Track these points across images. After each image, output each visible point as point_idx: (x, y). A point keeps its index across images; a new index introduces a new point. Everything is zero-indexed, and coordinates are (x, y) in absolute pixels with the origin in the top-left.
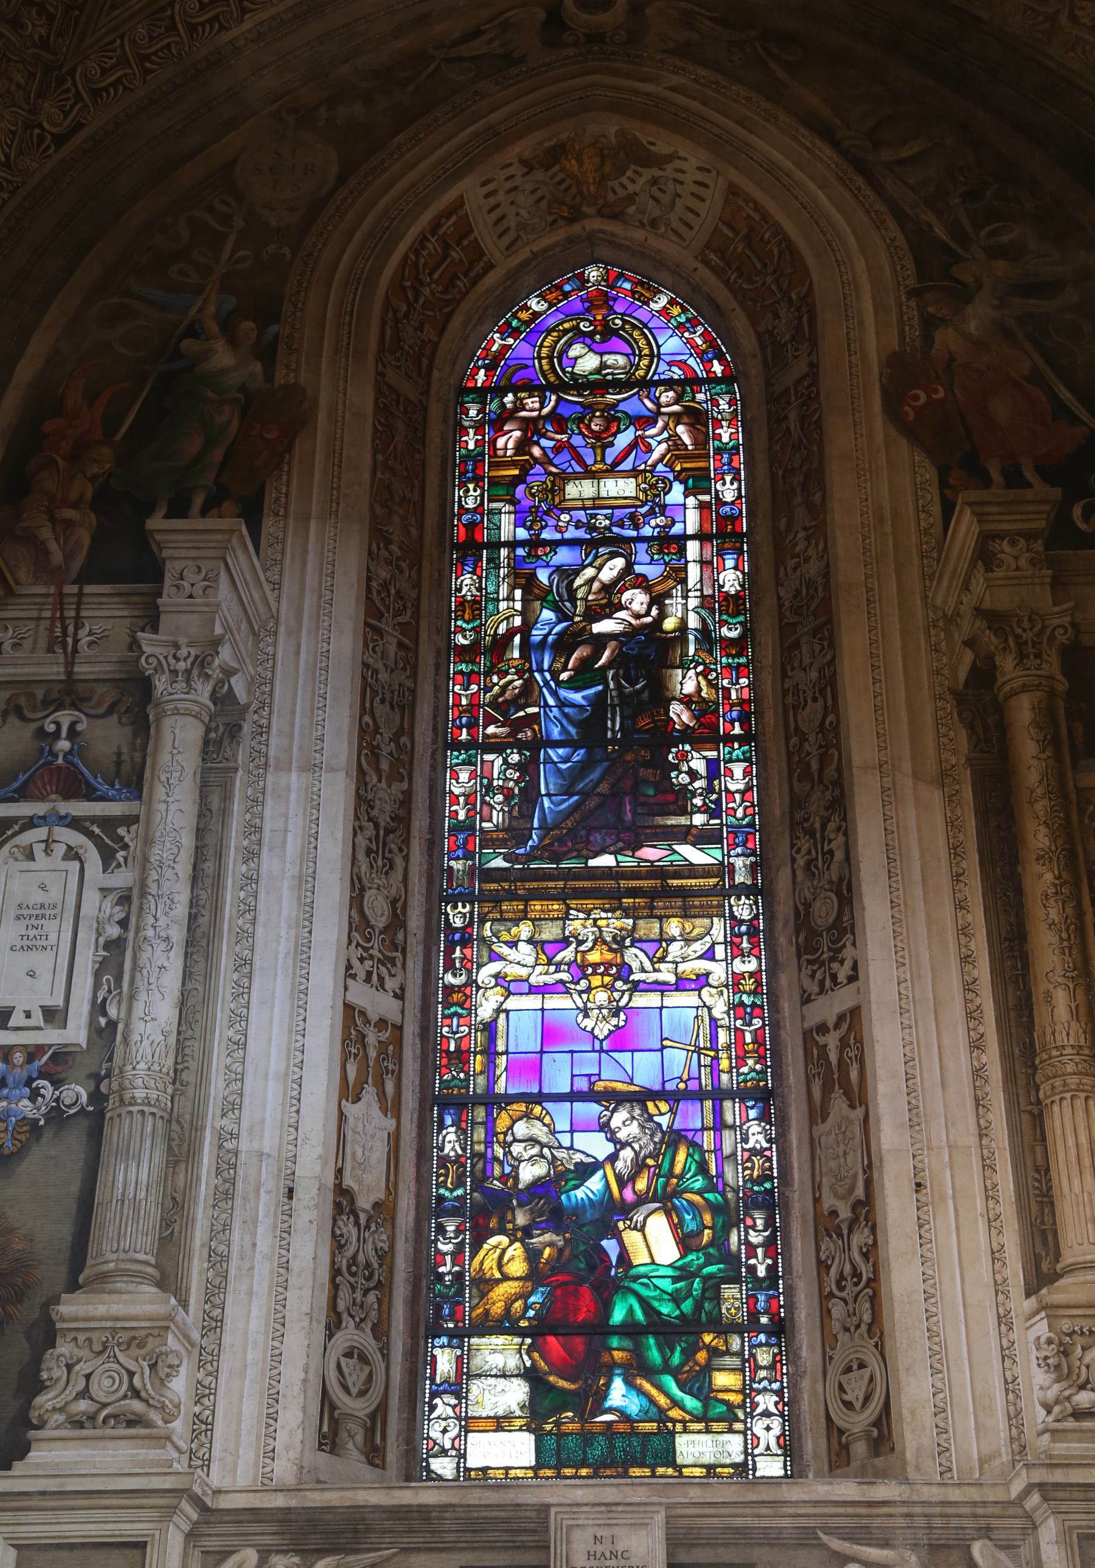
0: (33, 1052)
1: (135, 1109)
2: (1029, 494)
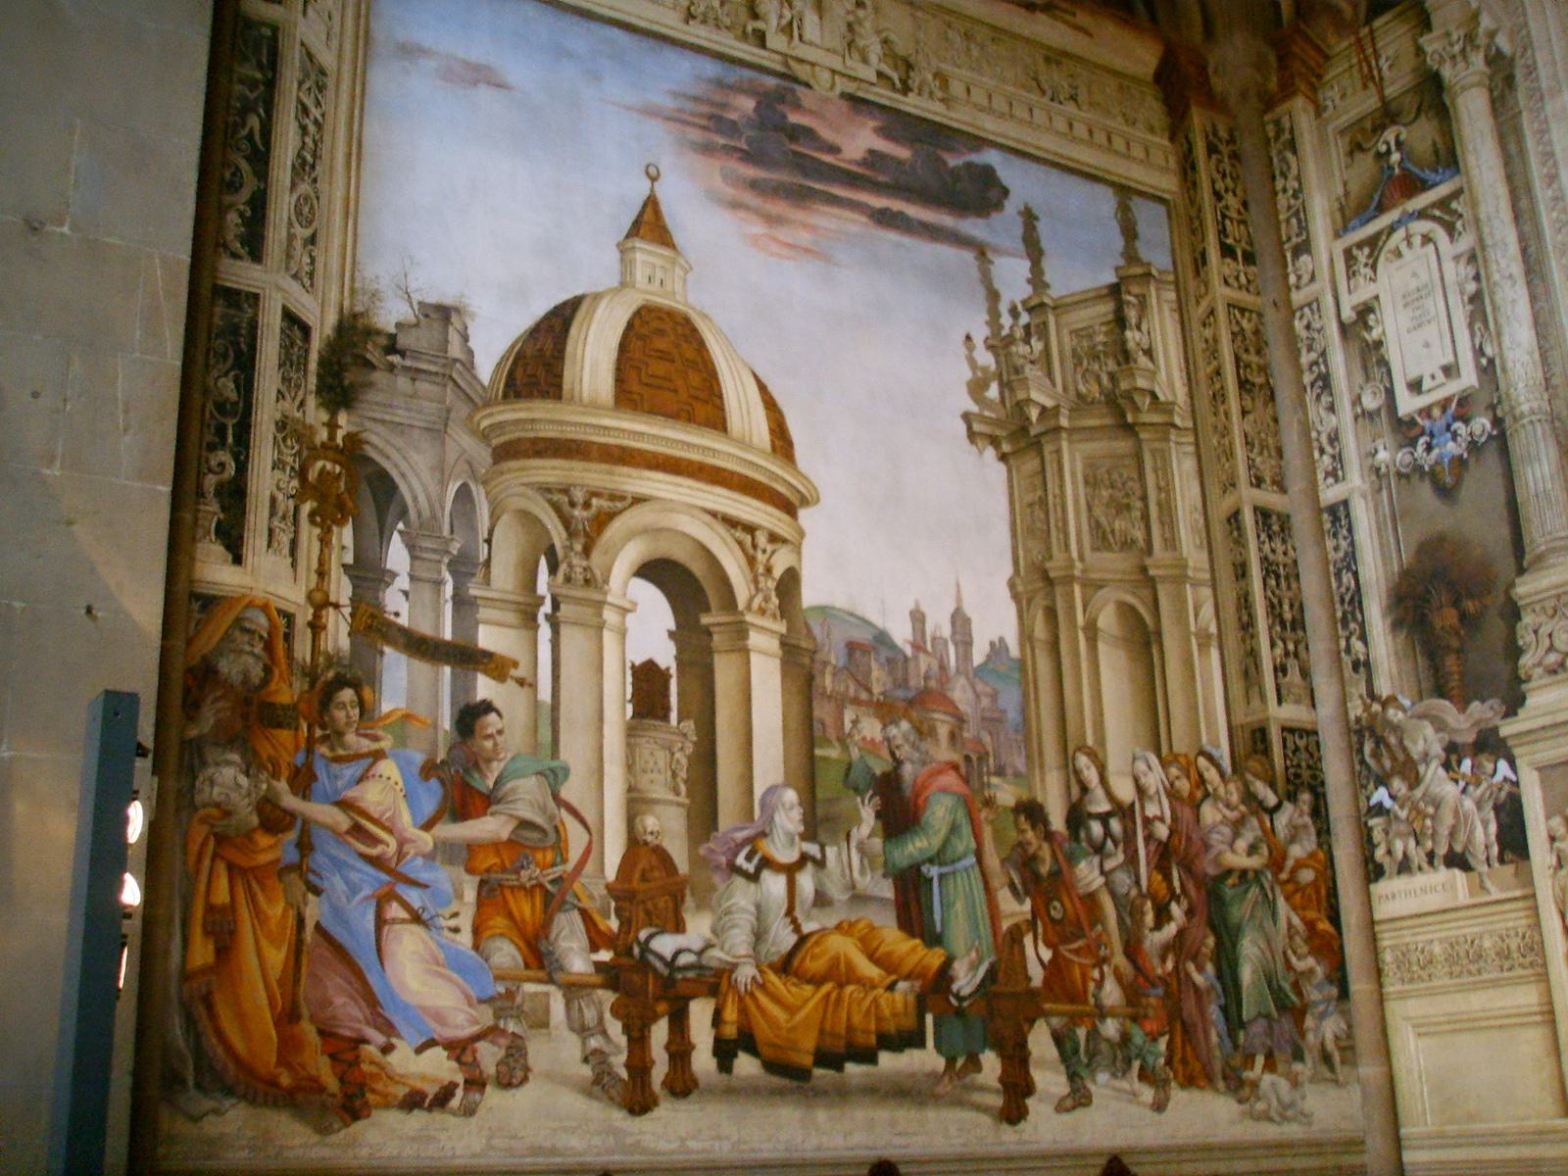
0: (1444, 405)
1: (1525, 421)
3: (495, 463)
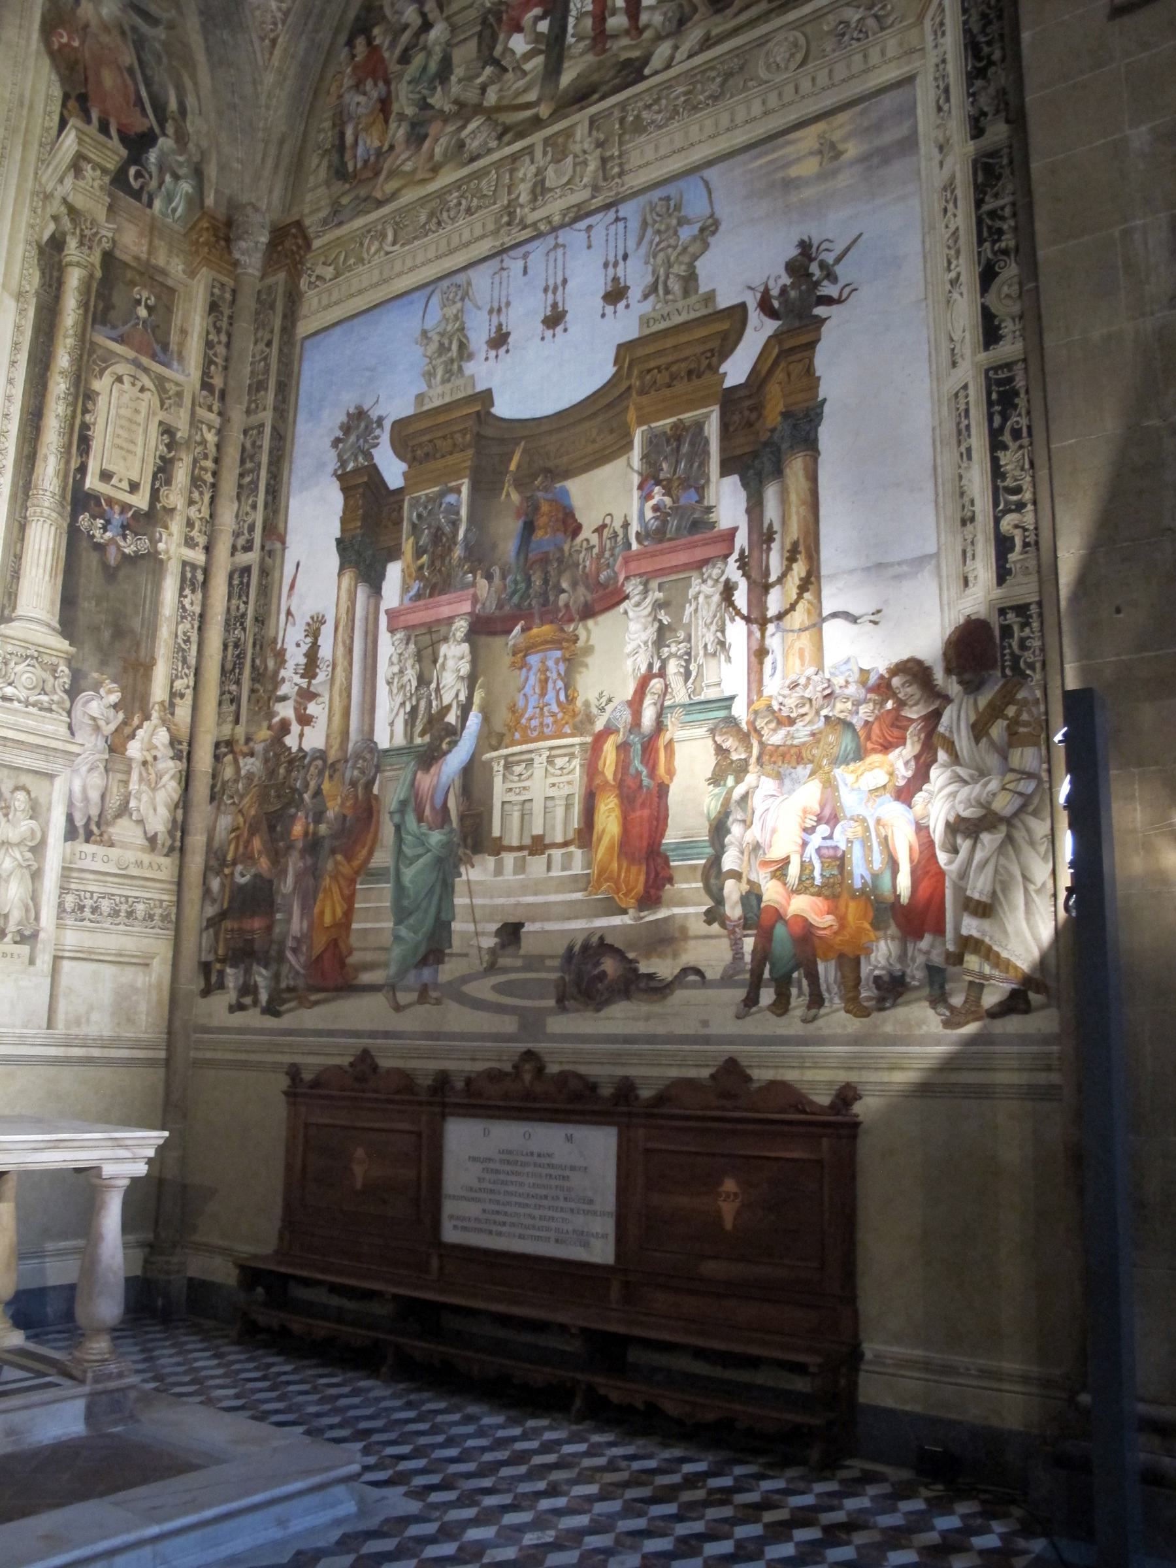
2: (110, 143)
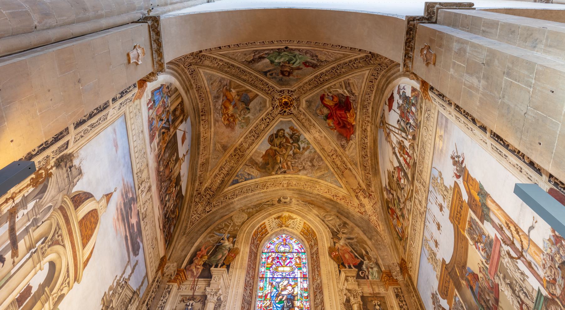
2: (352, 270)
3: (59, 208)
